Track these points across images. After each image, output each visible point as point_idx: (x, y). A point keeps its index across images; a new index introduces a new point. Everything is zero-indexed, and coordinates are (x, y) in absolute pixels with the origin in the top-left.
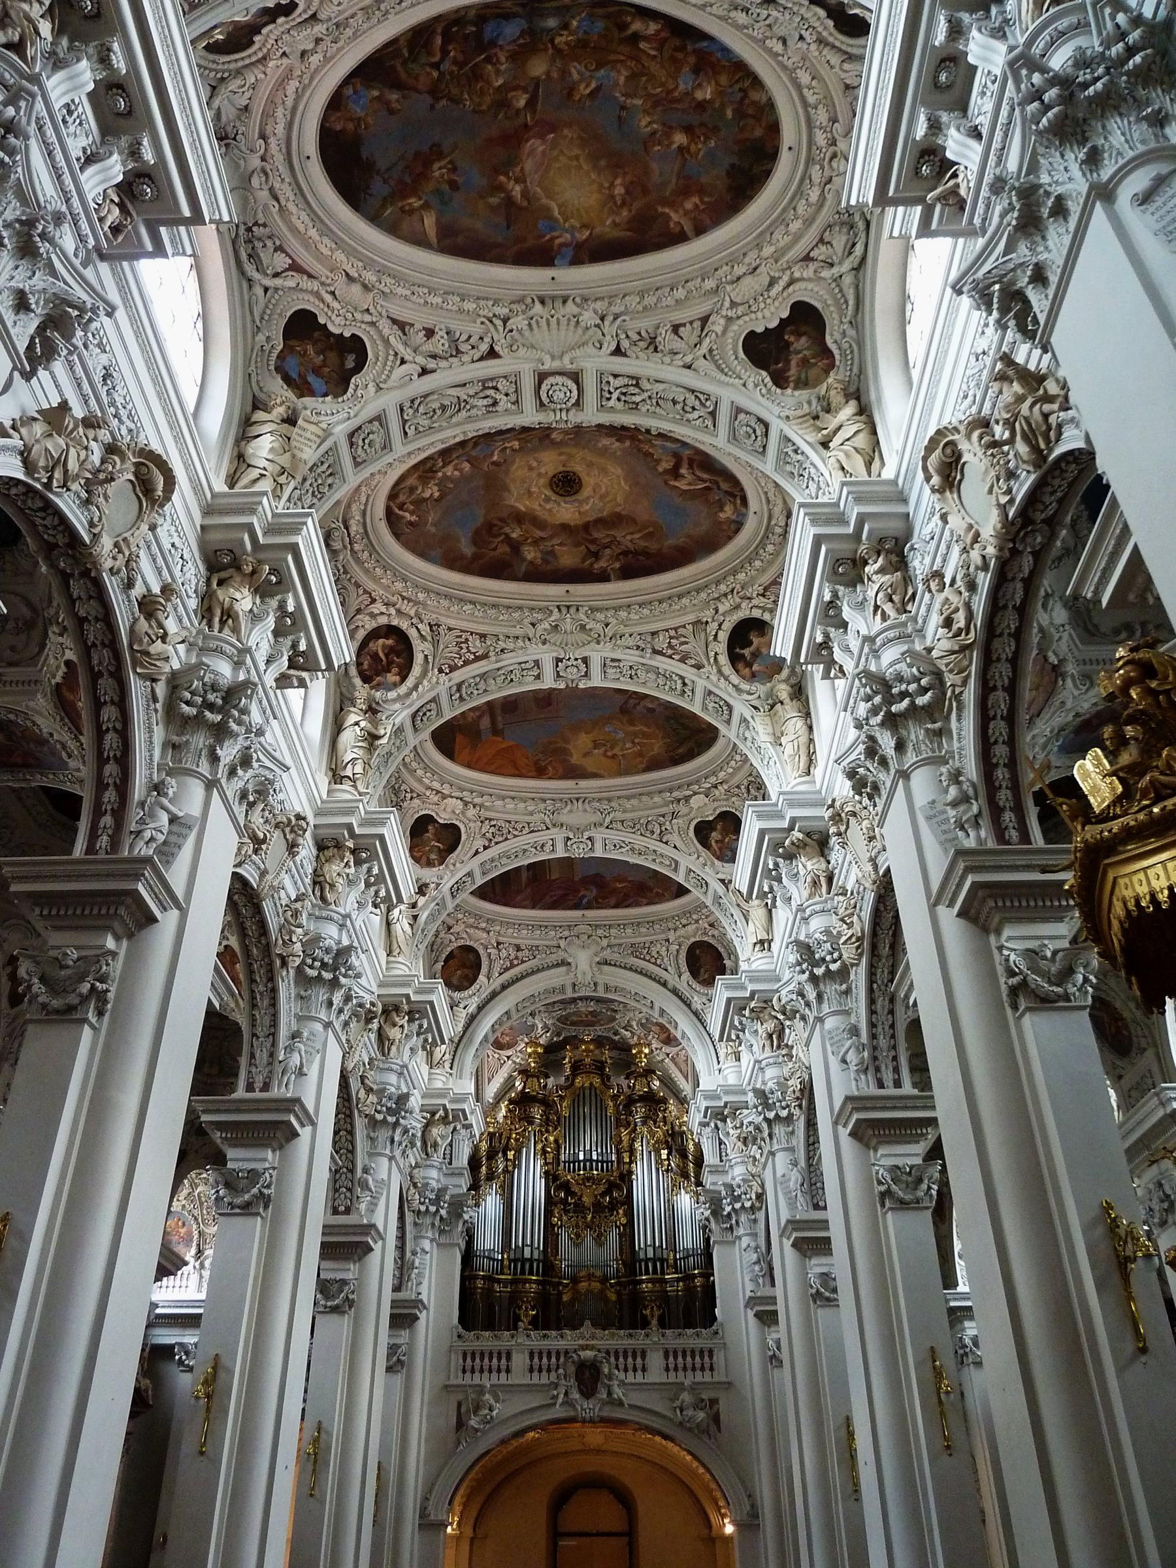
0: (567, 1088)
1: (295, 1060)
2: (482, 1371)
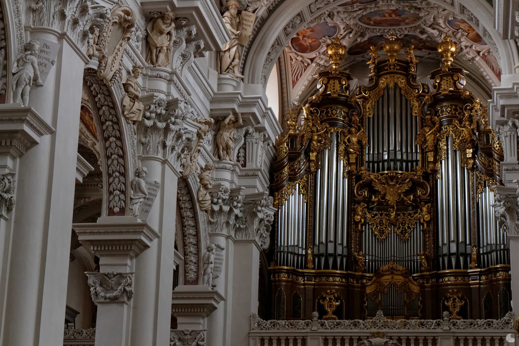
0: (371, 89)
1: (29, 72)
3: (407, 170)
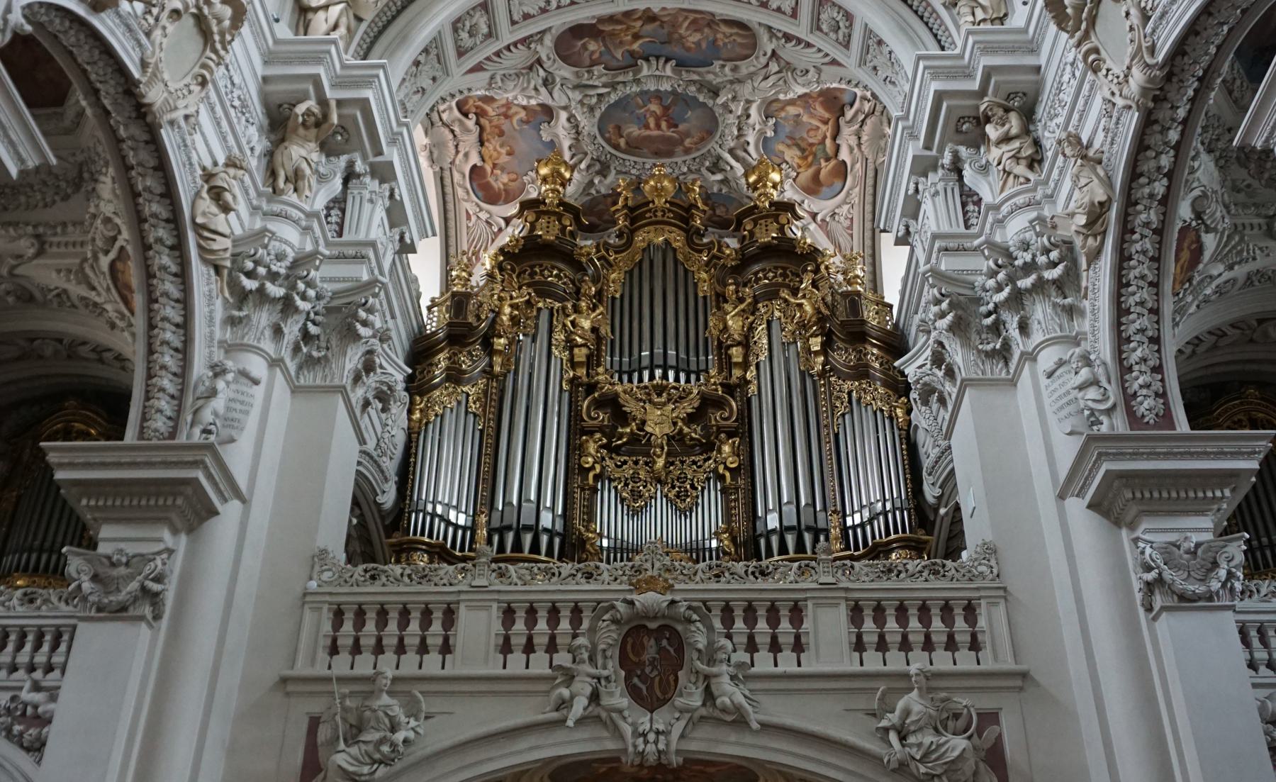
2: (379, 649)
3: (688, 381)
